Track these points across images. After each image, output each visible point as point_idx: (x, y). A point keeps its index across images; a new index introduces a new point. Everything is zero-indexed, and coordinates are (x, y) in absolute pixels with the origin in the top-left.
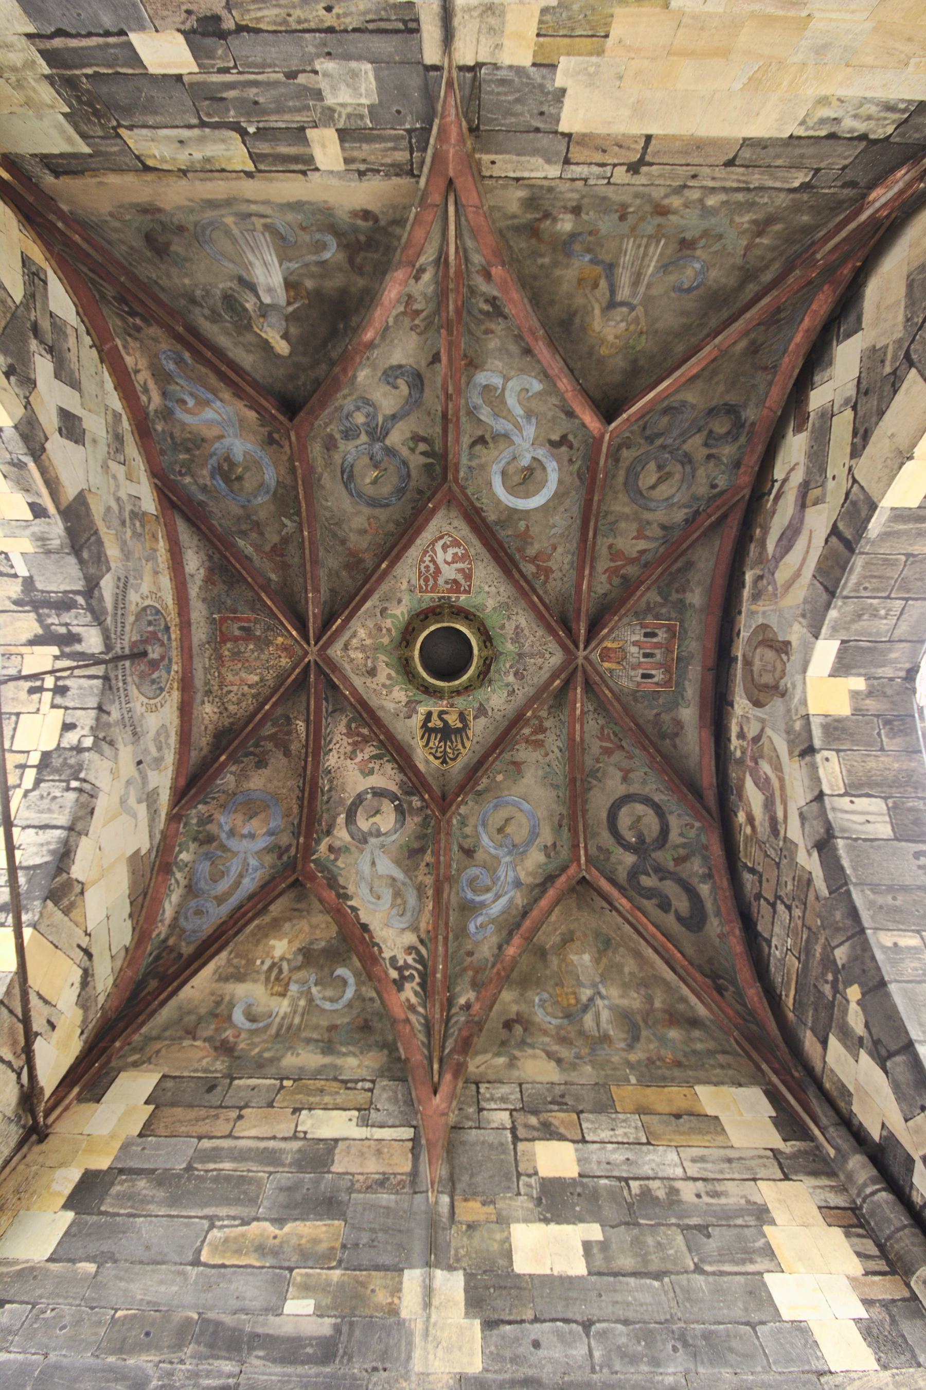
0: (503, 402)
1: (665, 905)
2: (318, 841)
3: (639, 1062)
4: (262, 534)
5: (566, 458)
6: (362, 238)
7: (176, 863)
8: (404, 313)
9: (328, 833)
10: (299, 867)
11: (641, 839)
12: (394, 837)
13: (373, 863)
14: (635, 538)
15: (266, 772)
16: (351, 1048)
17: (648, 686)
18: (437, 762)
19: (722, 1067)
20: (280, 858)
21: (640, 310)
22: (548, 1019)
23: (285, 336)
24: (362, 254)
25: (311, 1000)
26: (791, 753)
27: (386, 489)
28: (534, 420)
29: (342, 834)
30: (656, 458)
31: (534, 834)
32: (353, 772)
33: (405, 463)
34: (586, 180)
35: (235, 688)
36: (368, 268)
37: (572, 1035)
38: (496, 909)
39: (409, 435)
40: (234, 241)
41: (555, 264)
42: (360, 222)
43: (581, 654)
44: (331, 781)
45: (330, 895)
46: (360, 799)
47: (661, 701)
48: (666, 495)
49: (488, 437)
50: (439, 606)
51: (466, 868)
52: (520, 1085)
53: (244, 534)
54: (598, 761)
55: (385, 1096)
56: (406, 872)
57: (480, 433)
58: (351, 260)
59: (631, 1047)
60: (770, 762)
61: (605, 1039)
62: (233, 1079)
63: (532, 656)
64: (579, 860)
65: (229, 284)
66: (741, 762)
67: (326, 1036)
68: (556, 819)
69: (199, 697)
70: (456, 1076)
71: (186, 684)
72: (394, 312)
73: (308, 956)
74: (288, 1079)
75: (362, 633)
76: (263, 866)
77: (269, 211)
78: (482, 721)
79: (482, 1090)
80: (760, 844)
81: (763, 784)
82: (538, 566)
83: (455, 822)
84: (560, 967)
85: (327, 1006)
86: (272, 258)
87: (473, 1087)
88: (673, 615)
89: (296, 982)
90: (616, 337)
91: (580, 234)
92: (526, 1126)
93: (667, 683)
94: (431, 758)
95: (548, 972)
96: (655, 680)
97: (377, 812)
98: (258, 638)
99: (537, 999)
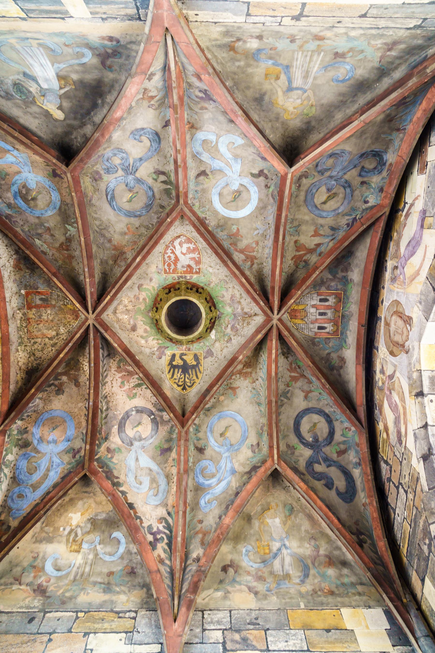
1: (329, 485)
2: (99, 446)
3: (307, 592)
5: (263, 184)
6: (110, 51)
7: (4, 463)
8: (143, 99)
9: (106, 439)
10: (86, 466)
11: (316, 440)
12: (151, 441)
13: (137, 459)
14: (313, 236)
15: (63, 397)
16: (123, 588)
17: (323, 334)
18: (180, 389)
19: (359, 594)
20: (74, 457)
21: (310, 93)
22: (251, 564)
23: (60, 108)
24: (110, 60)
25: (96, 555)
26: (410, 392)
28: (239, 161)
29: (115, 440)
30: (326, 184)
31: (245, 438)
32: (123, 395)
34: (264, 24)
35: (39, 340)
36: (116, 67)
37: (266, 575)
38: (219, 489)
40: (18, 52)
41: (248, 65)
42: (106, 42)
43: (276, 317)
44: (107, 403)
45: (108, 484)
46: (127, 415)
47: (331, 344)
48: (333, 208)
49: (208, 172)
50: (178, 283)
51: (199, 461)
52: (230, 611)
53: (40, 236)
54: (288, 386)
55: (144, 622)
57: (202, 169)
58: (103, 63)
59: (303, 582)
60: (398, 394)
61: (287, 576)
62: (46, 613)
64: (273, 457)
65: (17, 77)
66: (381, 389)
67: (106, 580)
70: (189, 608)
72: (136, 99)
73: (94, 524)
74: (81, 611)
75: (126, 301)
76: (62, 462)
77: (40, 36)
78: (210, 359)
79: (205, 616)
80: (392, 447)
81: (394, 408)
83: (191, 429)
84: (260, 528)
85: (107, 558)
87: (200, 614)
88: (339, 287)
90: (295, 108)
91: (264, 49)
92: (233, 641)
93: (335, 333)
94: (175, 386)
95: (252, 531)
96: (327, 330)
97: (139, 424)
99: (244, 550)
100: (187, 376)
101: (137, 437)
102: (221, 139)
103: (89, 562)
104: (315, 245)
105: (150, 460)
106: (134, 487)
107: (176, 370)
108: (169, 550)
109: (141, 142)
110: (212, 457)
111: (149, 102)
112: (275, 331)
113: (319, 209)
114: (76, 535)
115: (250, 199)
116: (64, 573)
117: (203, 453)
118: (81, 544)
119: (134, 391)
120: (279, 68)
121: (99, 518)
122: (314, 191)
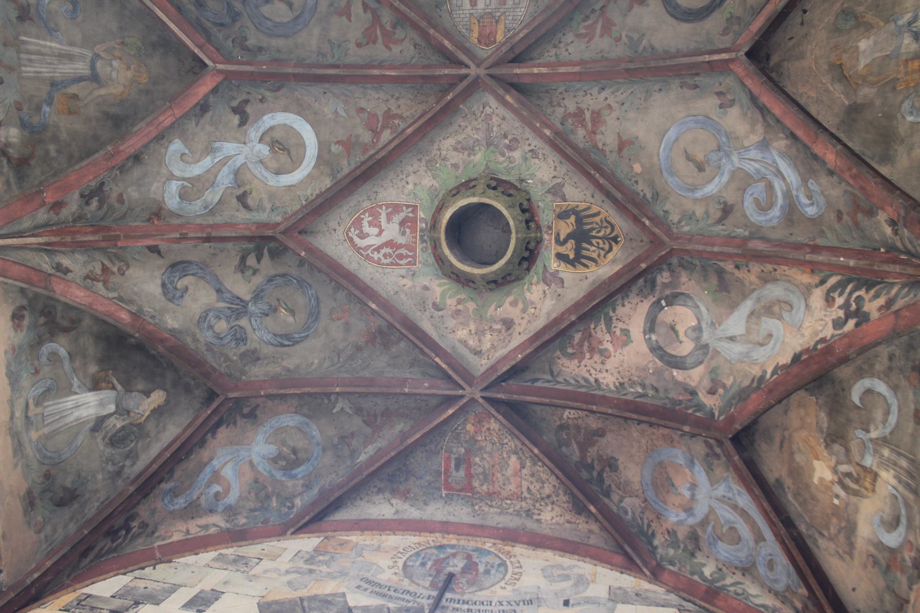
0: (198, 178)
2: (700, 407)
4: (352, 435)
5: (260, 106)
6: (42, 320)
7: (713, 581)
8: (105, 283)
9: (693, 393)
13: (732, 339)
15: (622, 460)
18: (615, 248)
20: (717, 456)
21: (99, 49)
23: (147, 394)
24: (59, 320)
25: (885, 441)
27: (300, 300)
28: (217, 144)
29: (696, 376)
30: (257, 7)
31: (706, 122)
33: (270, 280)
35: (525, 484)
38: (792, 176)
39: (239, 275)
40: (55, 433)
41: (55, 139)
42: (26, 322)
43: (473, 71)
44: (633, 384)
46: (657, 350)
53: (353, 454)
54: (618, 39)
56: (745, 296)
57: (235, 200)
58: (66, 330)
63: (489, 130)
65: (99, 440)
68: (688, 93)
69: (531, 525)
71: (510, 536)
72: (103, 292)
73: (836, 437)
75: (462, 333)
76: (725, 480)
77: (22, 401)
78: (569, 190)
82: (384, 127)
85: (893, 419)
86: (70, 401)
89: (863, 457)
90: (128, 68)
91: (21, 119)
94: (610, 256)
95: (878, 102)
97: (673, 328)
98: (468, 451)
99: (910, 119)
100: (594, 233)
101: (695, 335)
102: (177, 173)
103: (894, 457)
104: (365, 12)
105: (736, 314)
106: (773, 348)
107: (584, 253)
108: (878, 287)
109: (187, 289)
110: (739, 189)
111: (113, 273)
112: (496, 71)
113: (302, 13)
114: (848, 475)
115: (285, 125)
116: (903, 512)
117: (732, 206)
118: (864, 468)
119: (618, 333)
120: (57, 96)
121: (825, 425)
122: (269, 23)
